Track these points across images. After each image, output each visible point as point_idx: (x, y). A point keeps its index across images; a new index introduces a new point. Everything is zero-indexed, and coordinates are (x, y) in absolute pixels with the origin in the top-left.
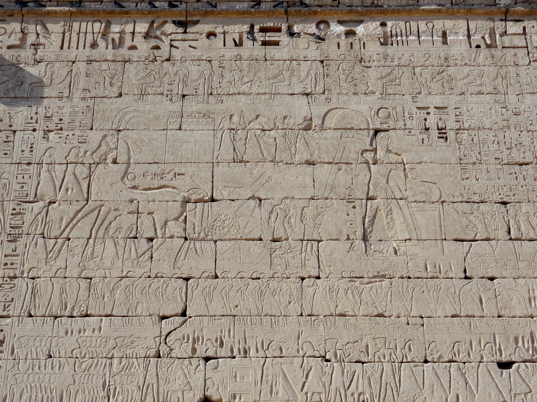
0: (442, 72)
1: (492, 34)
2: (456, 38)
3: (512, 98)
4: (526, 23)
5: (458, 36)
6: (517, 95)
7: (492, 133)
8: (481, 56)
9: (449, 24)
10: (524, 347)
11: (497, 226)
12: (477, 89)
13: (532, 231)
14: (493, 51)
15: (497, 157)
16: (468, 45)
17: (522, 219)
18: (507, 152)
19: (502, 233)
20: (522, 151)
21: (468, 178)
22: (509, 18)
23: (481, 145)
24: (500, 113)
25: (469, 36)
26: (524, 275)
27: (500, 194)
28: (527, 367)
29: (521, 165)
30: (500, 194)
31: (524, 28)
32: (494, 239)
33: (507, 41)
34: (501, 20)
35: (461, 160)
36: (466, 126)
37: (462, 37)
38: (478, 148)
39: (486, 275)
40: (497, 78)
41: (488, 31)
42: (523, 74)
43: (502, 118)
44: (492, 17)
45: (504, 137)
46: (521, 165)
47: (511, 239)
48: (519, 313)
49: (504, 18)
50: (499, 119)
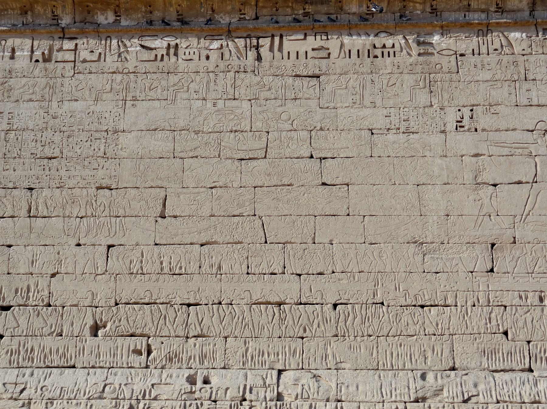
0: (5, 83)
1: (51, 50)
2: (21, 53)
3: (54, 104)
4: (77, 41)
5: (23, 52)
6: (58, 102)
7: (33, 134)
8: (38, 69)
9: (18, 41)
10: (21, 295)
11: (21, 207)
12: (29, 97)
13: (46, 210)
14: (47, 65)
15: (33, 152)
16: (29, 60)
17: (41, 201)
18: (41, 148)
19: (24, 212)
20: (53, 147)
21: (8, 170)
22: (66, 36)
23: (23, 143)
24: (42, 117)
25: (32, 52)
26: (33, 243)
27: (29, 182)
28: (20, 309)
29: (50, 159)
30: (29, 182)
31: (76, 45)
32: (17, 217)
33: (60, 56)
34: (60, 38)
35: (5, 155)
36: (15, 127)
37: (27, 53)
38: (20, 146)
39: (5, 244)
40: (45, 88)
41: (48, 47)
42: (66, 84)
43: (43, 120)
44: (53, 35)
45: (42, 136)
46: (50, 159)
47: (30, 217)
48: (22, 271)
49: (62, 36)
50: (40, 123)
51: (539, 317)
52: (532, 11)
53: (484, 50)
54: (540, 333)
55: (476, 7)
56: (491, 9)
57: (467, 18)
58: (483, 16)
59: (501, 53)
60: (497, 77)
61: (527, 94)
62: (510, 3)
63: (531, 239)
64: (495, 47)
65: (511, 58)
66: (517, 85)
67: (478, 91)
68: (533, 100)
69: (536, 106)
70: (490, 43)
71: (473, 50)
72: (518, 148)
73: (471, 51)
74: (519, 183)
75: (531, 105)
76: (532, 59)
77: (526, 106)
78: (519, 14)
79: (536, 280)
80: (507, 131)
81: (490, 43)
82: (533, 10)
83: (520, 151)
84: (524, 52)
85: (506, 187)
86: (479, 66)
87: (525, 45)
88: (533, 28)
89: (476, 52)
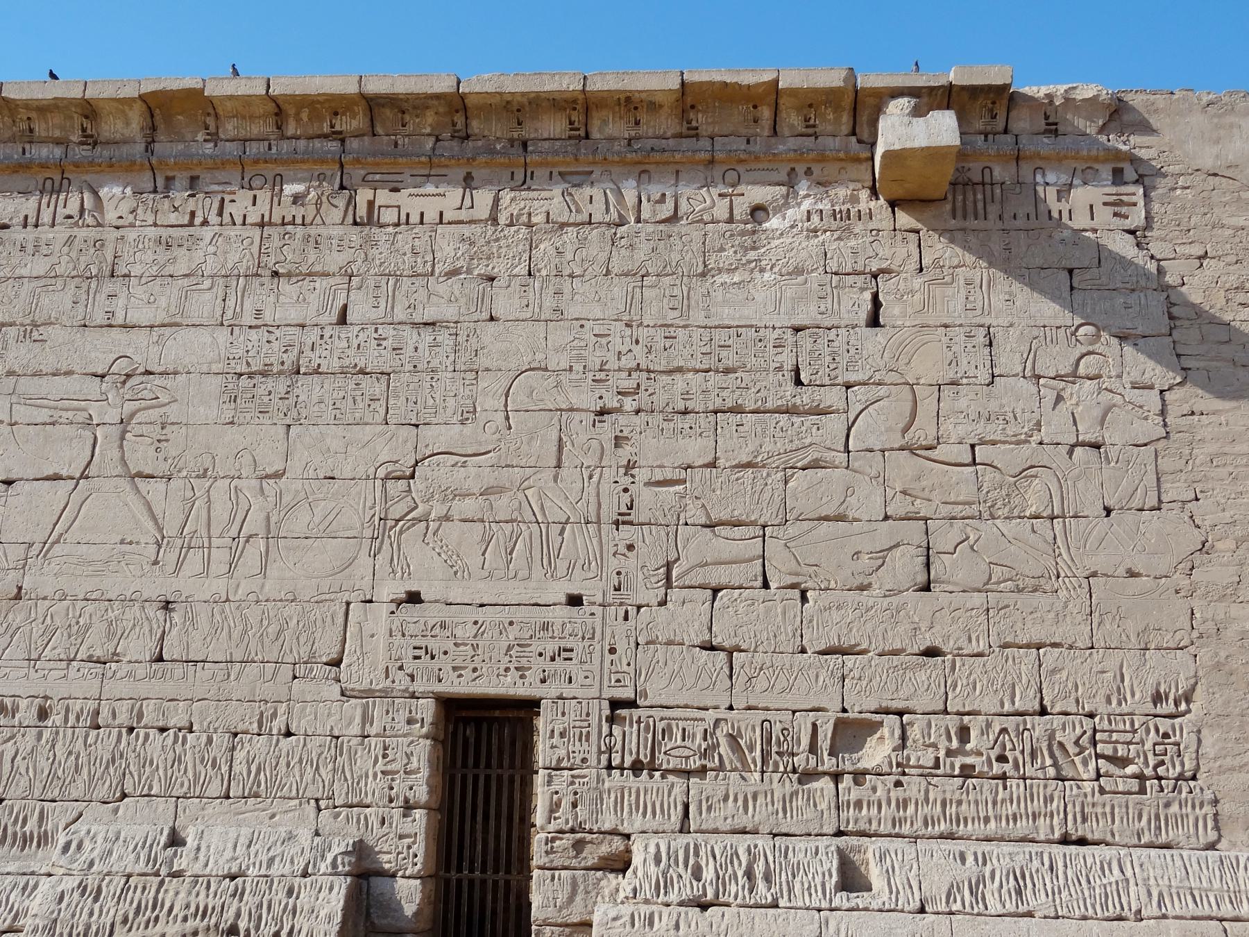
51: (29, 749)
52: (150, 143)
53: (46, 217)
54: (24, 782)
55: (43, 134)
56: (72, 138)
57: (28, 155)
58: (58, 152)
59: (76, 224)
60: (59, 270)
61: (107, 302)
62: (107, 128)
63: (48, 591)
64: (67, 212)
65: (93, 233)
66: (93, 286)
67: (17, 295)
68: (117, 315)
69: (120, 326)
70: (61, 203)
71: (26, 217)
72: (67, 410)
73: (22, 218)
74: (56, 477)
75: (110, 326)
76: (131, 235)
77: (101, 327)
78: (125, 149)
79: (41, 673)
80: (54, 375)
81: (61, 203)
82: (154, 141)
83: (70, 414)
84: (120, 222)
85: (28, 486)
86: (30, 248)
87: (124, 208)
88: (149, 174)
89: (31, 220)
